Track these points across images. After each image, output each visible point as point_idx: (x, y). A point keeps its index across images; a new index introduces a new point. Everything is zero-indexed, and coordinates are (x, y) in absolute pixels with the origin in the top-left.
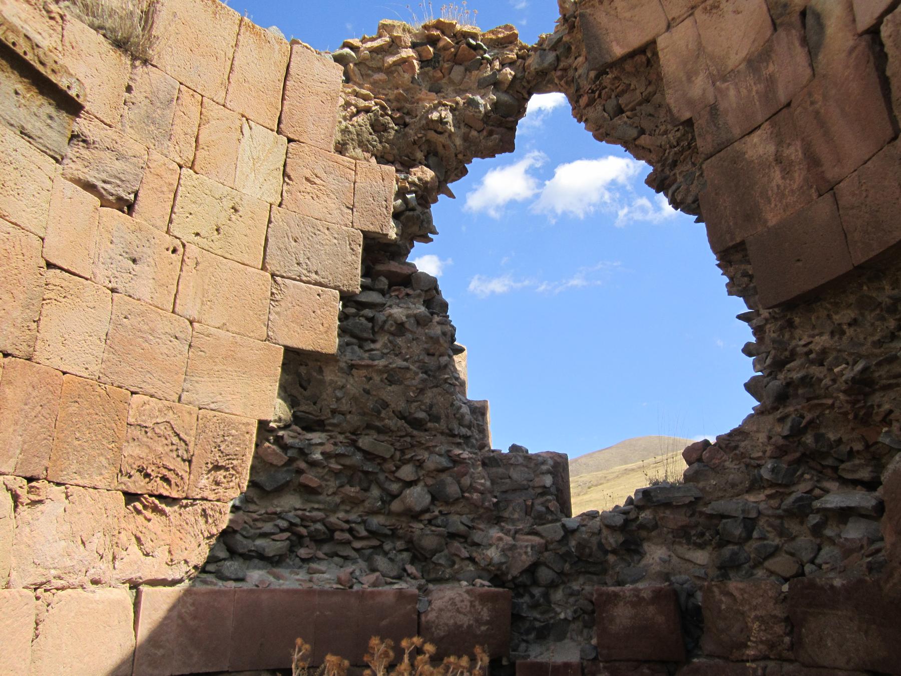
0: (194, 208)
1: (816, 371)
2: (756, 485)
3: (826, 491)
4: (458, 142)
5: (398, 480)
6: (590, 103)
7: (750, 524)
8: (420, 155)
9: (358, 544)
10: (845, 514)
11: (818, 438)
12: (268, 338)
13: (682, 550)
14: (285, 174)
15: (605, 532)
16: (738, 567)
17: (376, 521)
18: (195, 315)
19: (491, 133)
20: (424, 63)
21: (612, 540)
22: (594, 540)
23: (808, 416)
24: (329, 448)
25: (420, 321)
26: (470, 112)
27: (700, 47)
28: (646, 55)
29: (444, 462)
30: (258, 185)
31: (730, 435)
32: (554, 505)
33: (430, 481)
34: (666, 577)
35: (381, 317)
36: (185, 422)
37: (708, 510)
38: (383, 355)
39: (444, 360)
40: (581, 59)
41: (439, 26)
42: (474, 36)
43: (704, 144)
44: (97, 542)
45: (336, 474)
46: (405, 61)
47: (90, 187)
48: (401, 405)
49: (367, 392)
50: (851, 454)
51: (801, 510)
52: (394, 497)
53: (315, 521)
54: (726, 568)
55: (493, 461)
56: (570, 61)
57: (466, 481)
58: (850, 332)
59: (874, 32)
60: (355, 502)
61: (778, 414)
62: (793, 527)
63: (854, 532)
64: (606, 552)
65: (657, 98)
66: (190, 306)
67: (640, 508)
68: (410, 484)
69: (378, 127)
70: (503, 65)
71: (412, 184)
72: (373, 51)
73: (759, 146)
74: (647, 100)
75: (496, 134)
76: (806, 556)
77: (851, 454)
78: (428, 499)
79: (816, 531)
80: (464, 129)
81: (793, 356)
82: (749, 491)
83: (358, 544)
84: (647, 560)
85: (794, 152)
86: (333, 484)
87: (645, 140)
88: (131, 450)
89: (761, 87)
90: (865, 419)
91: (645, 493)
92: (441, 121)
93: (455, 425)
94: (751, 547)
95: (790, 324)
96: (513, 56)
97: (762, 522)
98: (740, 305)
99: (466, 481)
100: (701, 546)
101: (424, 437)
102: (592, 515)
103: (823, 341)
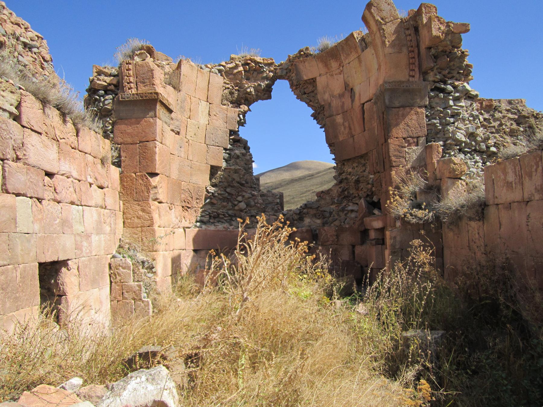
0: (191, 130)
1: (349, 177)
3: (349, 205)
4: (255, 96)
5: (237, 200)
6: (296, 89)
7: (331, 213)
8: (243, 101)
9: (226, 219)
10: (352, 211)
11: (348, 193)
12: (207, 163)
13: (314, 219)
14: (209, 114)
15: (294, 215)
16: (327, 223)
17: (230, 212)
18: (191, 159)
19: (265, 94)
20: (245, 71)
21: (296, 217)
22: (291, 217)
23: (346, 187)
24: (219, 192)
25: (243, 155)
26: (259, 88)
27: (328, 85)
28: (313, 81)
29: (250, 195)
30: (203, 119)
31: (328, 190)
32: (280, 208)
33: (246, 201)
34: (310, 226)
35: (233, 153)
36: (191, 188)
37: (321, 209)
38: (233, 165)
39: (250, 166)
40: (294, 74)
41: (250, 60)
42: (261, 63)
43: (327, 114)
44: (179, 218)
45: (220, 199)
46: (241, 72)
47: (173, 130)
48: (238, 180)
49: (229, 176)
50: (355, 197)
51: (343, 210)
52: (236, 205)
53: (214, 212)
54: (324, 224)
55: (262, 195)
56: (291, 74)
57: (256, 201)
58: (356, 169)
59: (364, 104)
60: (224, 207)
61: (340, 186)
62: (341, 213)
63: (353, 215)
64: (294, 220)
65: (315, 92)
66: (190, 158)
67: (304, 209)
68: (240, 202)
69: (231, 93)
70: (269, 72)
71: (242, 112)
72: (230, 68)
73: (339, 119)
74: (313, 92)
75: (266, 93)
76: (343, 221)
77: (355, 197)
78: (245, 206)
79: (346, 215)
80: (256, 93)
81: (344, 172)
82: (332, 205)
83: (226, 219)
84: (305, 222)
85: (346, 124)
86: (219, 202)
87: (311, 103)
88: (183, 196)
89: (341, 104)
90: (357, 189)
91: (306, 205)
92: (251, 92)
93: (252, 185)
94: (331, 219)
95: (344, 164)
96: (272, 69)
97: (334, 213)
98: (333, 156)
99: (256, 201)
100: (319, 219)
101: (244, 188)
102: (291, 210)
103: (350, 170)
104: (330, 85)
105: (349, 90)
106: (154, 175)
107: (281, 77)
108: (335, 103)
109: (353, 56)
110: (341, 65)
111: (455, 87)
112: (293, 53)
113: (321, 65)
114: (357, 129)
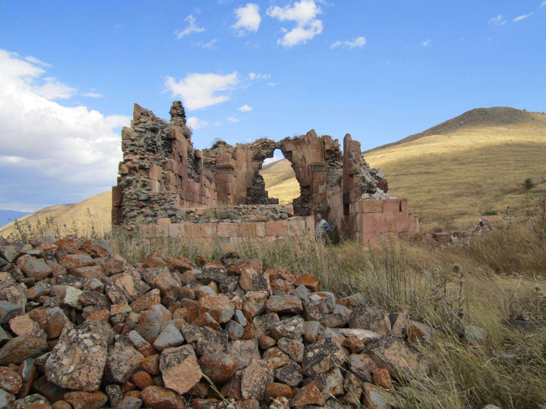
7: (298, 208)
25: (261, 182)
28: (291, 152)
30: (244, 169)
73: (301, 170)
104: (297, 154)
105: (304, 158)
106: (229, 194)
108: (299, 162)
109: (305, 146)
110: (301, 148)
111: (337, 164)
112: (283, 138)
113: (294, 146)
114: (307, 175)
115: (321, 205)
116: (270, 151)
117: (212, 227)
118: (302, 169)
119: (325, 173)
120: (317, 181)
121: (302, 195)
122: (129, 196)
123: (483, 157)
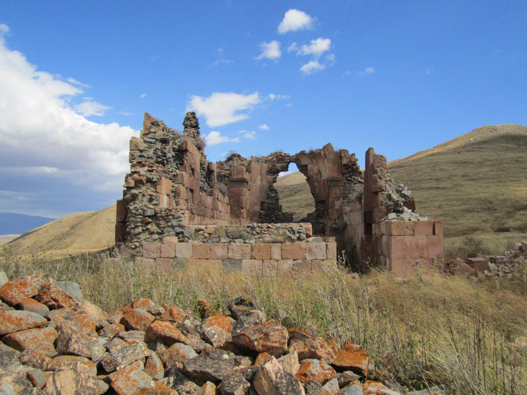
2: (314, 219)
25: (275, 196)
28: (306, 166)
30: (259, 183)
55: (283, 214)
73: (316, 184)
104: (312, 168)
105: (319, 172)
106: (242, 208)
107: (293, 162)
108: (315, 177)
109: (321, 160)
110: (317, 162)
111: (355, 179)
113: (309, 160)
114: (322, 190)
115: (337, 221)
116: (285, 165)
117: (222, 248)
118: (318, 184)
119: (342, 188)
120: (334, 196)
121: (316, 210)
122: (134, 212)
123: (494, 173)
